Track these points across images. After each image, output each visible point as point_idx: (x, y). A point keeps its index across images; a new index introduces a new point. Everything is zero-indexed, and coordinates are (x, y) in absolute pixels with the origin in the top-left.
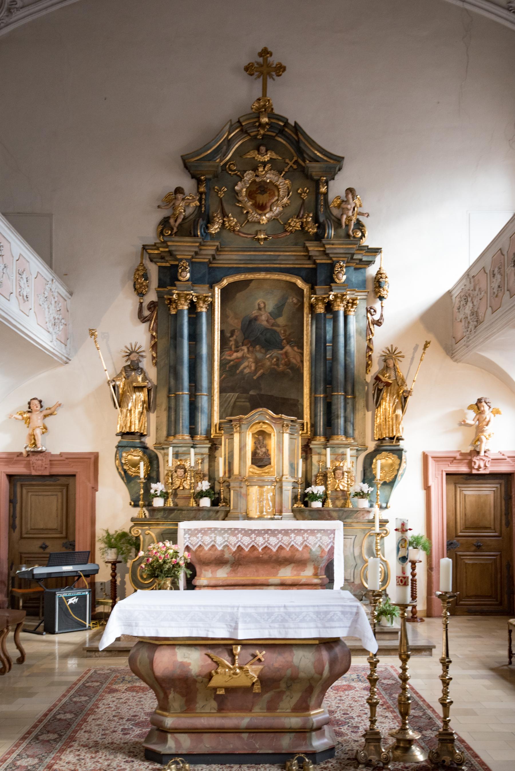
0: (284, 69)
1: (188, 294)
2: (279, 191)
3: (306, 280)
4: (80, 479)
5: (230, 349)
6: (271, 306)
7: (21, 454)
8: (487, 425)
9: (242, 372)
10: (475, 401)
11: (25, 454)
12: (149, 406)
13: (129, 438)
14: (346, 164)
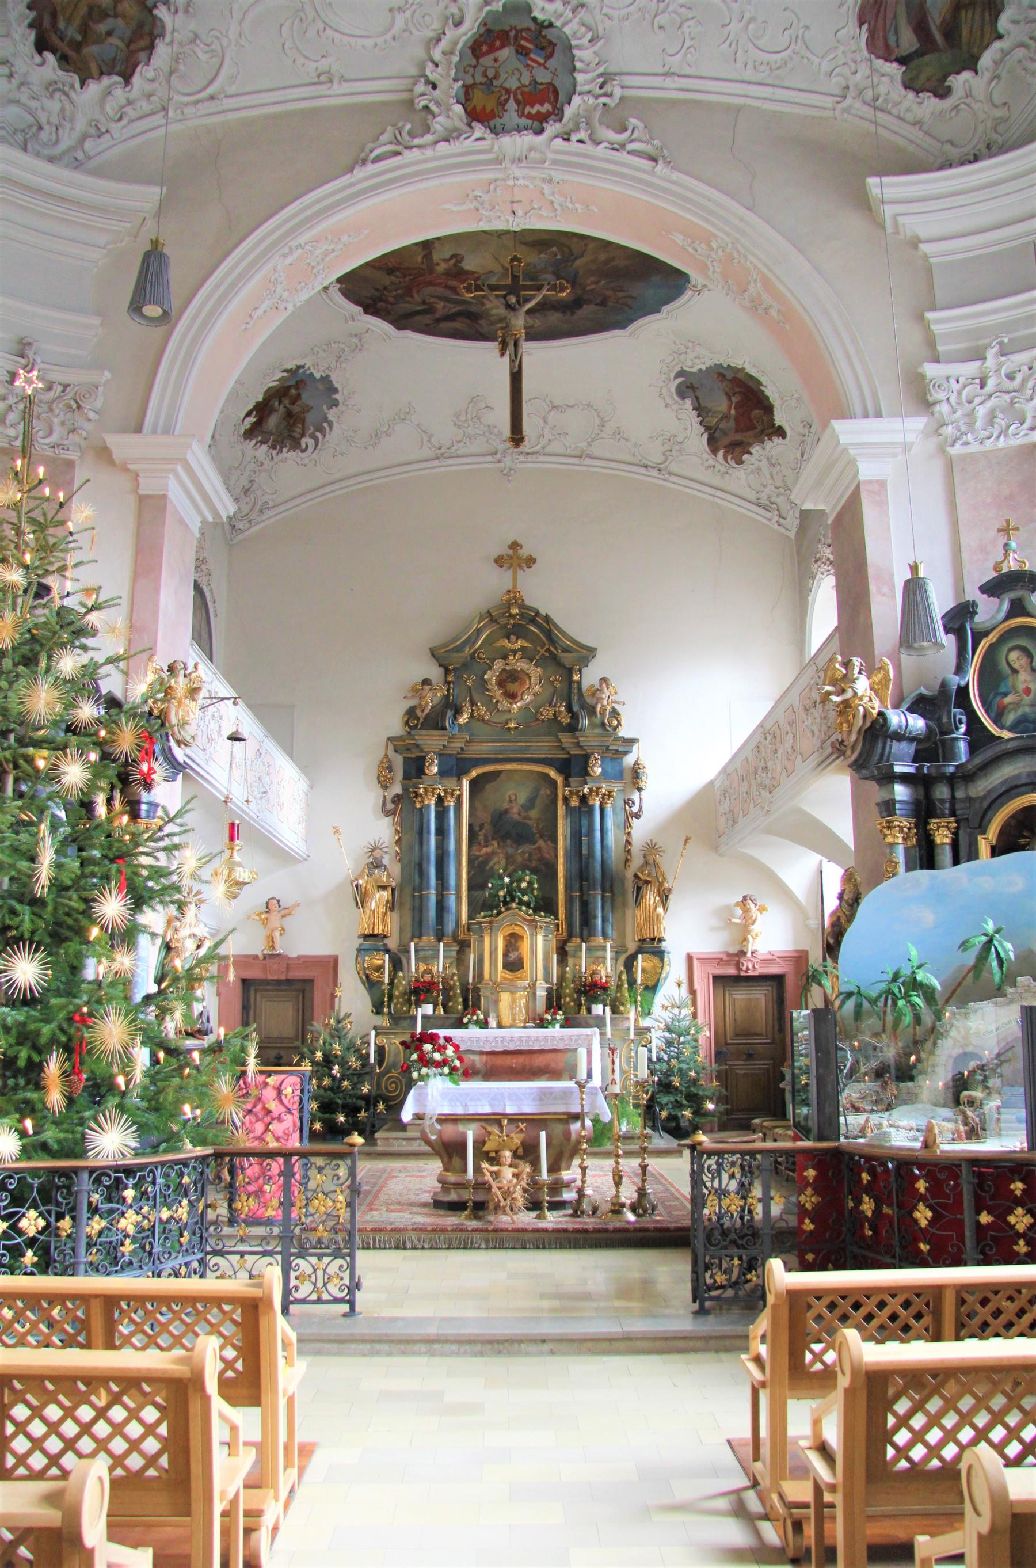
0: (534, 561)
3: (560, 771)
6: (522, 797)
7: (256, 957)
11: (261, 956)
12: (391, 906)
14: (600, 656)
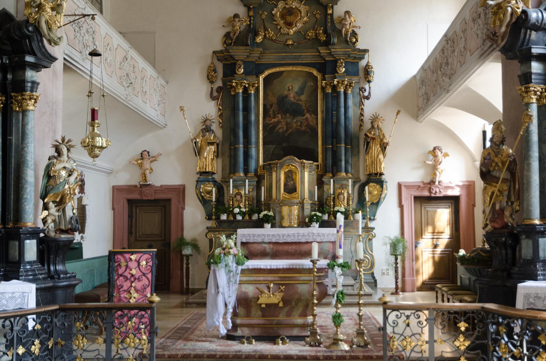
1: (242, 83)
2: (301, 13)
3: (319, 71)
4: (174, 202)
5: (270, 116)
6: (296, 88)
7: (136, 186)
8: (440, 164)
9: (278, 131)
10: (432, 149)
11: (139, 186)
12: (217, 155)
13: (204, 176)
